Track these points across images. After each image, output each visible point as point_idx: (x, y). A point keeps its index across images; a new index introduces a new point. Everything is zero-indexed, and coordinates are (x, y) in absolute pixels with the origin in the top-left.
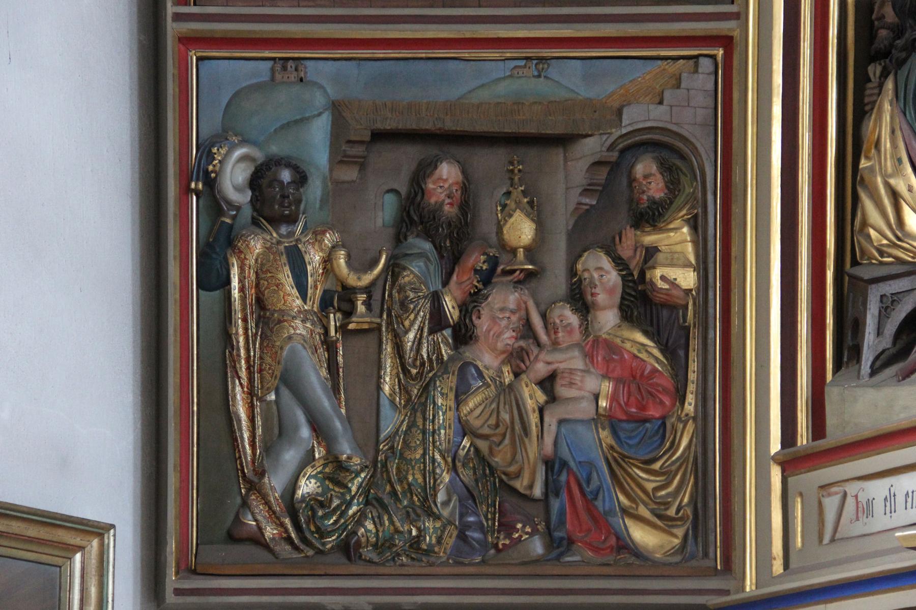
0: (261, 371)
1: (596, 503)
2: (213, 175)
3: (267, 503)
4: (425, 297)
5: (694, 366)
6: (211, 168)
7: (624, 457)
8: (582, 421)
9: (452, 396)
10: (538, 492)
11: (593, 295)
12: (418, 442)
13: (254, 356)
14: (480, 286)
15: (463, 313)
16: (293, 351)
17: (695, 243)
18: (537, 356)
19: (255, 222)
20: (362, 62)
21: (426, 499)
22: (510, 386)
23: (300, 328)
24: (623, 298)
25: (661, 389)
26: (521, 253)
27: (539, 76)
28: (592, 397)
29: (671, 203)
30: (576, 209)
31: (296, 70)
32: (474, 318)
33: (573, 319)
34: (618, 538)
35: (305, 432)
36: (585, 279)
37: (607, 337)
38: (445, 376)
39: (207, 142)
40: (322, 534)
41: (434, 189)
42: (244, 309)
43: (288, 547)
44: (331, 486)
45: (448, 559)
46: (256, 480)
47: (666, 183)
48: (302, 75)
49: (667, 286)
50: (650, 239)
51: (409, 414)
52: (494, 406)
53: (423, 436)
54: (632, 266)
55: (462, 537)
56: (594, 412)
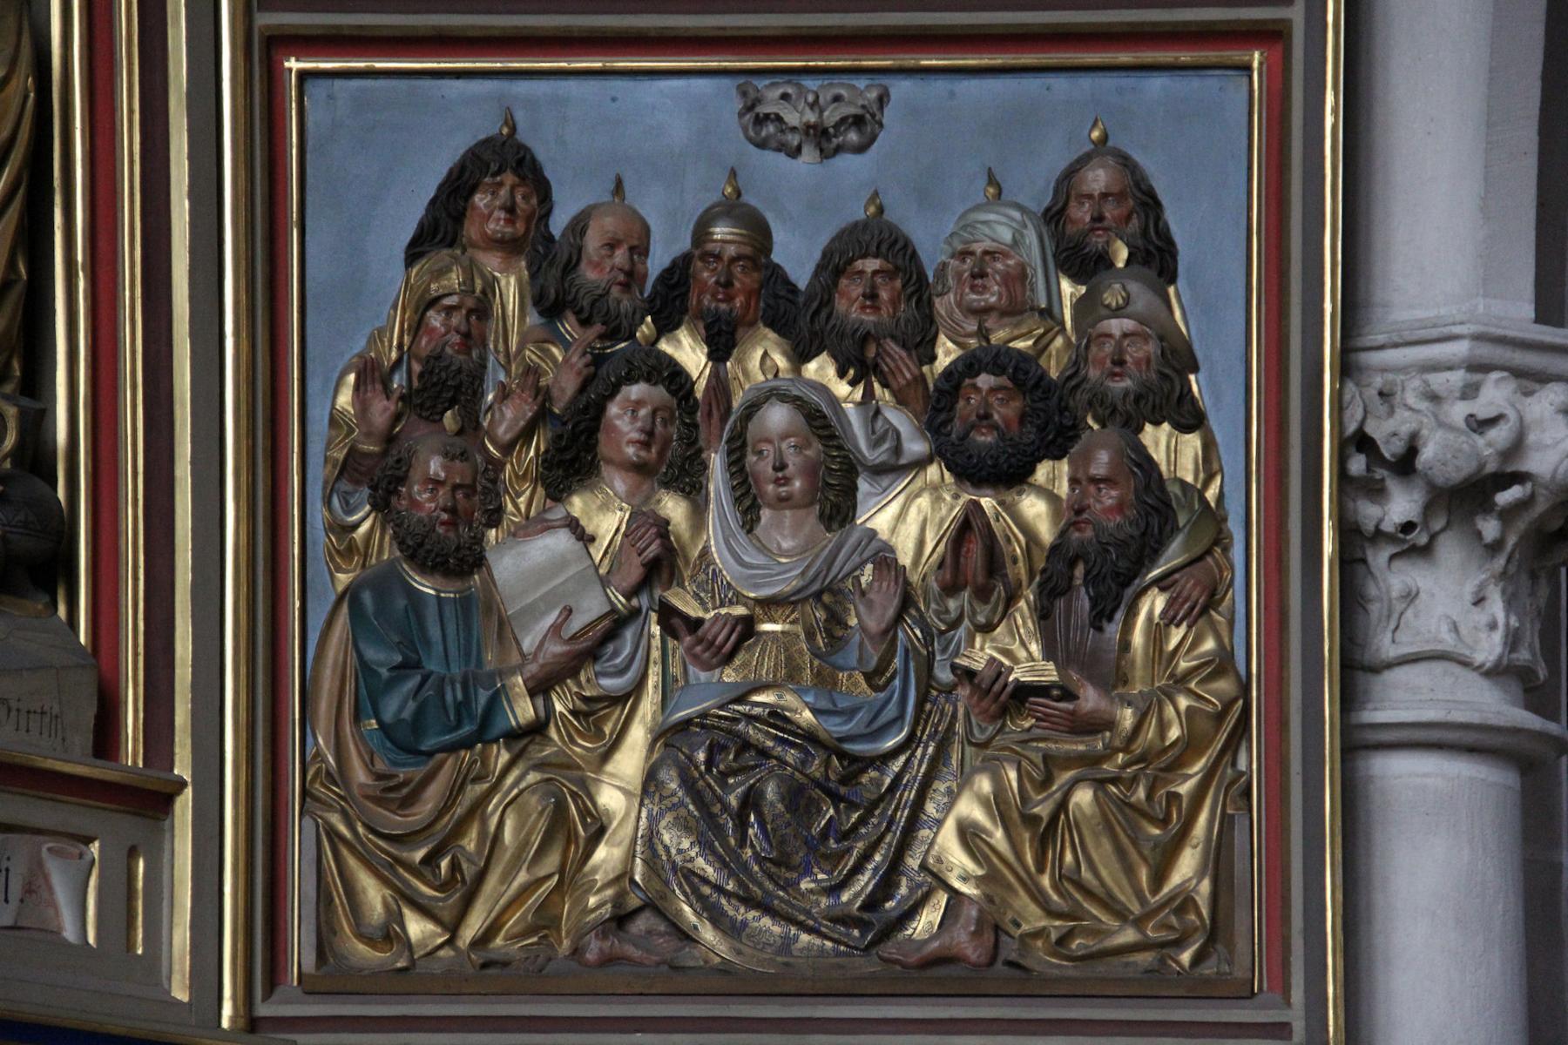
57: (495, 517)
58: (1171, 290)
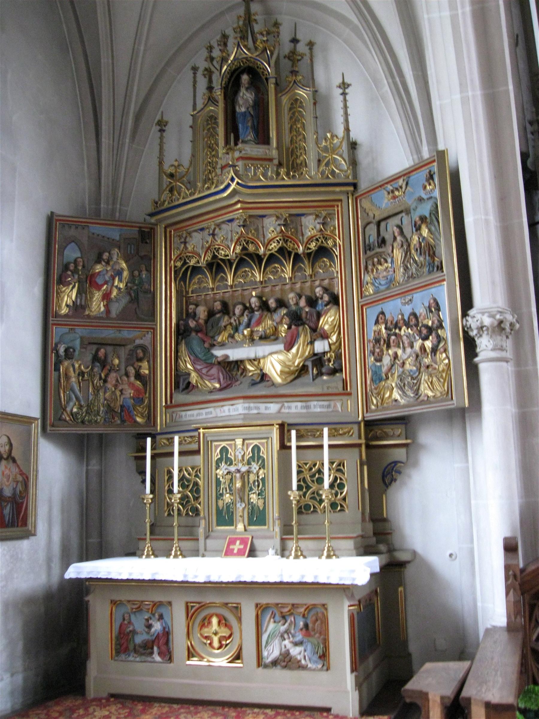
3: (67, 414)
10: (119, 411)
19: (65, 359)
23: (73, 379)
35: (74, 399)
40: (78, 419)
50: (140, 364)
55: (105, 420)
57: (383, 354)
58: (440, 313)
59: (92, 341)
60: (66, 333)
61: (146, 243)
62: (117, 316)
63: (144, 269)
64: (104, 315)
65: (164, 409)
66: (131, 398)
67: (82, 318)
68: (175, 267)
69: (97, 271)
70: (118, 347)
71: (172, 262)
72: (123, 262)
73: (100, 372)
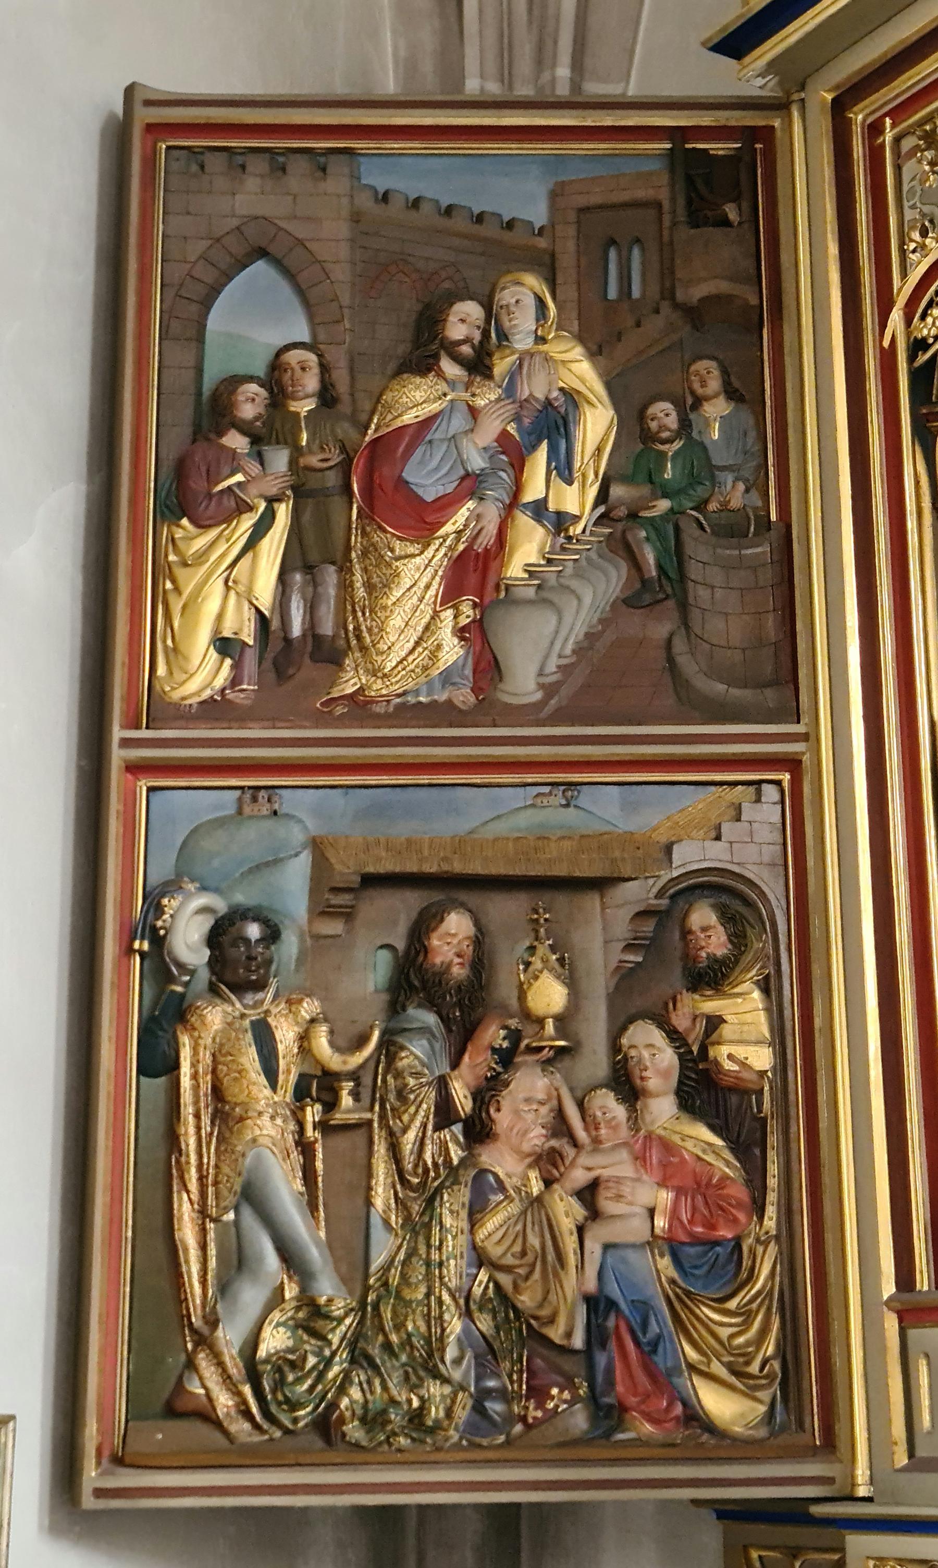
0: (216, 1183)
1: (656, 1359)
2: (162, 932)
3: (220, 1364)
4: (429, 1084)
5: (773, 1169)
6: (159, 923)
7: (688, 1293)
8: (633, 1246)
9: (464, 1214)
10: (578, 1341)
11: (642, 1078)
12: (420, 1277)
13: (208, 1163)
14: (500, 1069)
15: (478, 1104)
16: (258, 1158)
17: (768, 1010)
18: (574, 1159)
19: (213, 990)
20: (350, 791)
21: (430, 1355)
22: (539, 1200)
24: (680, 1082)
25: (734, 1202)
26: (550, 1024)
27: (567, 805)
28: (645, 1213)
29: (737, 962)
30: (618, 968)
31: (269, 800)
32: (492, 1111)
33: (619, 1111)
34: (685, 1404)
36: (632, 1057)
37: (662, 1133)
38: (456, 1188)
39: (156, 891)
40: (294, 1406)
41: (440, 946)
42: (196, 1102)
43: (247, 1426)
44: (305, 1337)
45: (461, 1438)
46: (205, 1330)
47: (729, 936)
48: (276, 806)
49: (736, 1068)
50: (711, 1006)
51: (408, 1237)
52: (519, 1227)
53: (427, 1270)
54: (690, 1042)
55: (479, 1408)
56: (649, 1232)
59: (388, 866)
60: (220, 823)
61: (725, 222)
62: (550, 690)
63: (714, 384)
64: (464, 696)
65: (891, 1323)
66: (654, 1240)
67: (322, 718)
68: (918, 345)
69: (408, 418)
70: (561, 900)
71: (896, 316)
72: (578, 352)
73: (444, 1068)
